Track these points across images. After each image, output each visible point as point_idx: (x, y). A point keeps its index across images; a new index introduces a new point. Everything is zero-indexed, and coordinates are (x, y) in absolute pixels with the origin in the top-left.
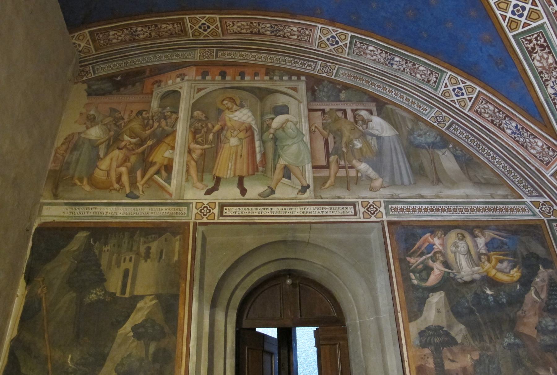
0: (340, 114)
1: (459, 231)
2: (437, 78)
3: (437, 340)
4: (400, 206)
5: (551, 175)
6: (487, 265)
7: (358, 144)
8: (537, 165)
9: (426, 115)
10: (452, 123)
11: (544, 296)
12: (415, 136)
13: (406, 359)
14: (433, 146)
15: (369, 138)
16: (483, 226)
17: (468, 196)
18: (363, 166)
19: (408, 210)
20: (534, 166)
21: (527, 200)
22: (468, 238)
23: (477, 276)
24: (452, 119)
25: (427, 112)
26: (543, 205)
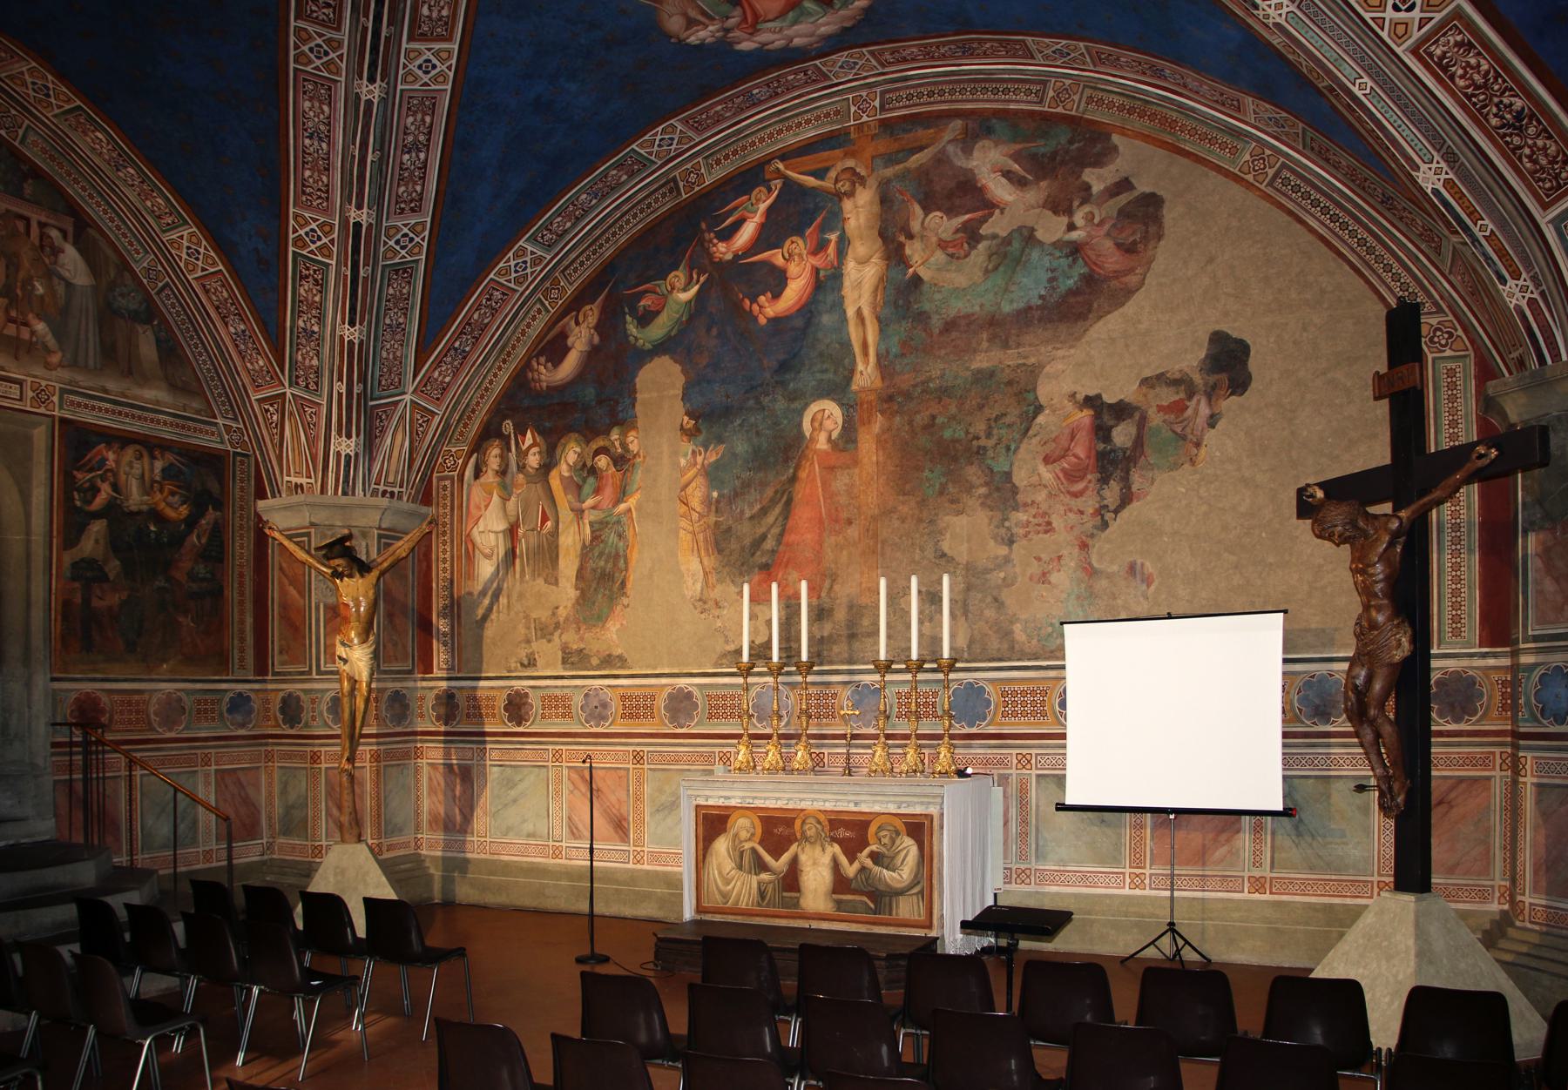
0: (21, 226)
1: (138, 447)
2: (173, 223)
3: (89, 574)
4: (78, 399)
5: (256, 400)
6: (158, 496)
7: (40, 289)
8: (247, 381)
9: (137, 262)
10: (167, 285)
11: (204, 541)
12: (116, 294)
13: (54, 591)
14: (135, 317)
15: (56, 281)
16: (163, 446)
17: (158, 402)
18: (40, 327)
19: (86, 406)
20: (242, 380)
21: (220, 421)
22: (146, 459)
23: (145, 508)
24: (167, 279)
25: (140, 256)
26: (235, 431)
